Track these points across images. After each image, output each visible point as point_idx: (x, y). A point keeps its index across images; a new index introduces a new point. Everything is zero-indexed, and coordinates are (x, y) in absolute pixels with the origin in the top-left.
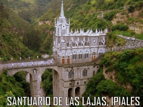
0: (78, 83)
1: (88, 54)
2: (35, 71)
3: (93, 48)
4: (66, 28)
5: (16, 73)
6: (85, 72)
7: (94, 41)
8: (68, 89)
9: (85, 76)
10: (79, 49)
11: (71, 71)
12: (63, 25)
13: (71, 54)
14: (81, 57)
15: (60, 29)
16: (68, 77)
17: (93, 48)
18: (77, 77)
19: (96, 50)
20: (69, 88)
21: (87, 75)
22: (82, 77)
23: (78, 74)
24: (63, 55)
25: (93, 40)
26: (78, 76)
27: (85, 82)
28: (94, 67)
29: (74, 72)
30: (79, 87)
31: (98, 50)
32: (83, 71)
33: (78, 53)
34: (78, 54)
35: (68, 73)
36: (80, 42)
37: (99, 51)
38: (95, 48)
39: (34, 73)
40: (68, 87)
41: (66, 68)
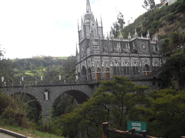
1: (137, 67)
2: (46, 94)
3: (144, 57)
7: (144, 47)
13: (112, 65)
14: (128, 71)
17: (144, 57)
19: (149, 62)
24: (98, 66)
25: (142, 45)
28: (154, 84)
31: (151, 62)
33: (122, 64)
34: (122, 66)
37: (153, 64)
39: (45, 98)
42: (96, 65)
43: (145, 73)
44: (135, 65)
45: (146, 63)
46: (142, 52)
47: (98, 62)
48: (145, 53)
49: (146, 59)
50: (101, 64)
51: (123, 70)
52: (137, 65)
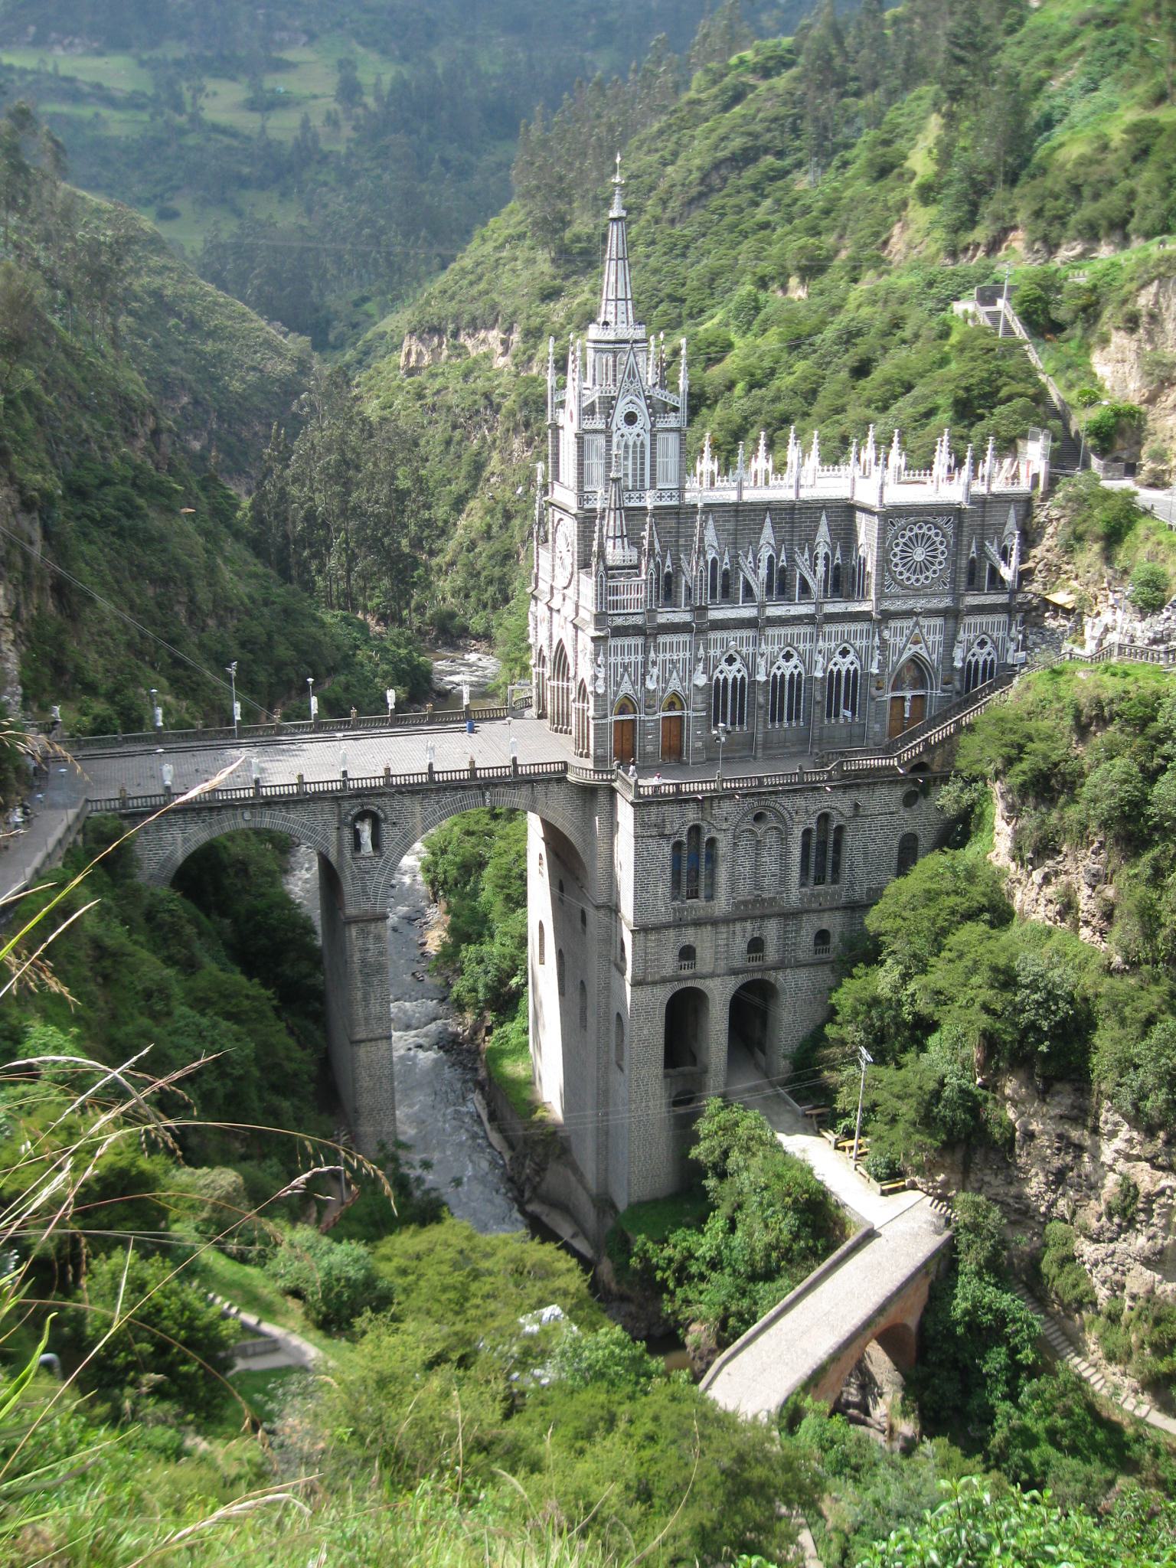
0: (756, 945)
1: (852, 678)
4: (653, 436)
5: (192, 847)
6: (822, 844)
7: (919, 554)
8: (664, 994)
9: (819, 880)
10: (770, 632)
11: (695, 830)
12: (621, 409)
13: (701, 680)
15: (601, 440)
16: (663, 889)
18: (745, 891)
20: (679, 986)
21: (845, 865)
22: (795, 894)
23: (757, 866)
24: (626, 688)
26: (758, 886)
27: (822, 937)
29: (723, 847)
30: (771, 976)
31: (950, 643)
32: (807, 833)
33: (762, 670)
35: (667, 850)
36: (782, 561)
37: (958, 653)
38: (923, 621)
39: (357, 845)
40: (664, 981)
41: (654, 809)
42: (618, 685)
43: (903, 698)
44: (844, 664)
45: (915, 648)
46: (900, 584)
47: (625, 667)
48: (916, 593)
49: (917, 624)
50: (644, 675)
51: (761, 700)
52: (857, 665)
